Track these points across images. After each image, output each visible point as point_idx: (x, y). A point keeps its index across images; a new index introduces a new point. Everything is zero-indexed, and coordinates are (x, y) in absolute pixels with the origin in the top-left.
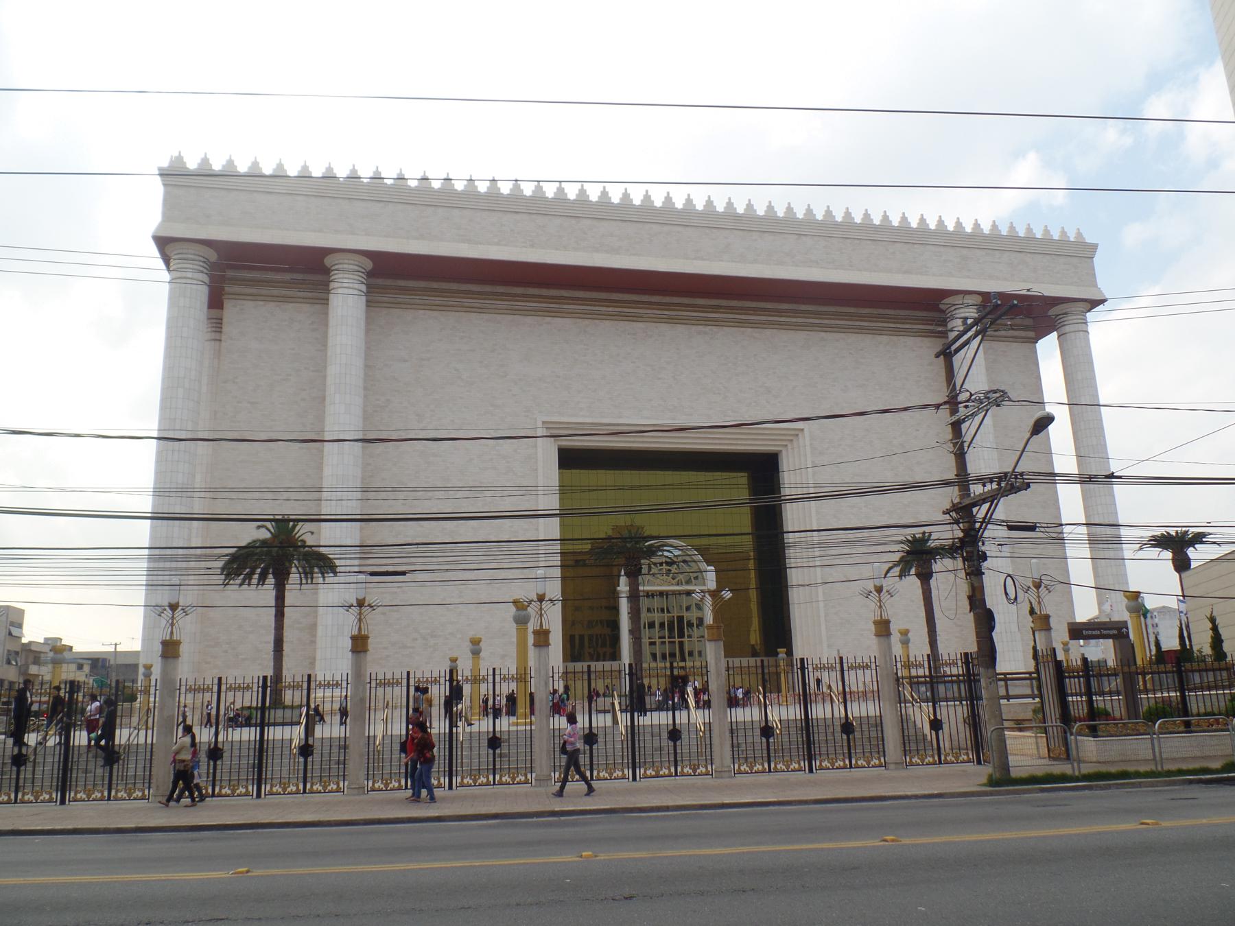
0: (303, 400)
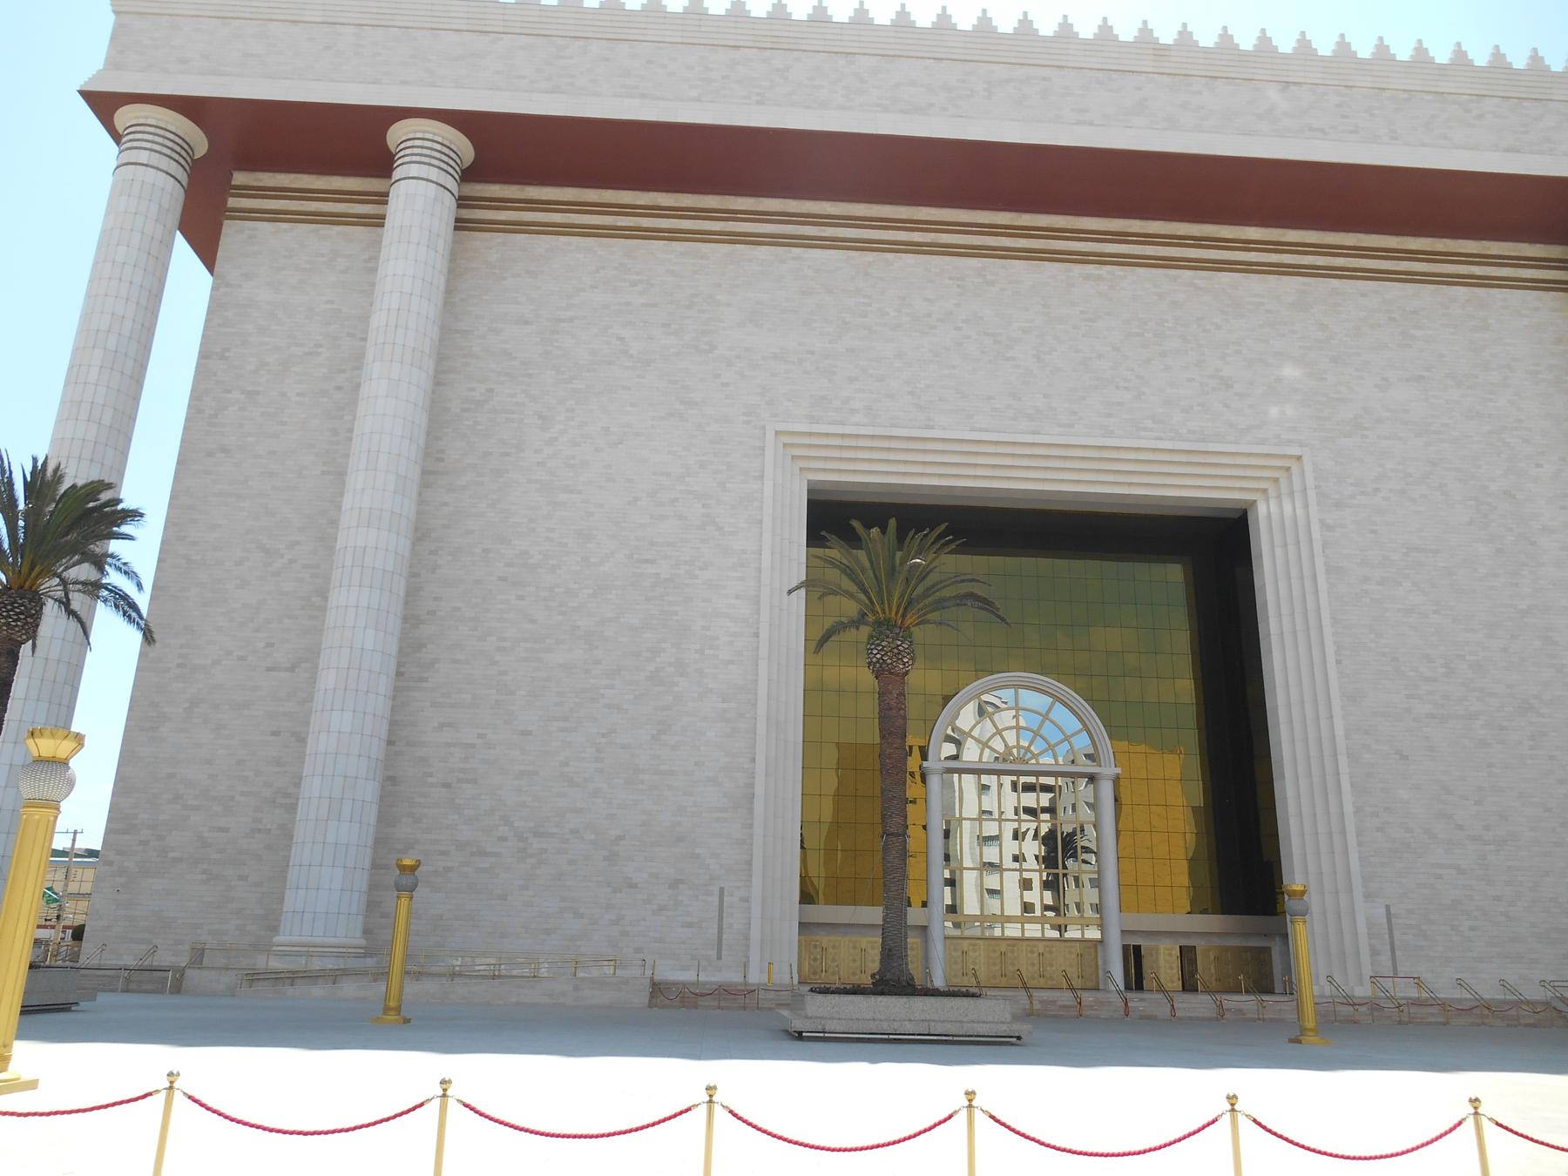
0: (339, 388)
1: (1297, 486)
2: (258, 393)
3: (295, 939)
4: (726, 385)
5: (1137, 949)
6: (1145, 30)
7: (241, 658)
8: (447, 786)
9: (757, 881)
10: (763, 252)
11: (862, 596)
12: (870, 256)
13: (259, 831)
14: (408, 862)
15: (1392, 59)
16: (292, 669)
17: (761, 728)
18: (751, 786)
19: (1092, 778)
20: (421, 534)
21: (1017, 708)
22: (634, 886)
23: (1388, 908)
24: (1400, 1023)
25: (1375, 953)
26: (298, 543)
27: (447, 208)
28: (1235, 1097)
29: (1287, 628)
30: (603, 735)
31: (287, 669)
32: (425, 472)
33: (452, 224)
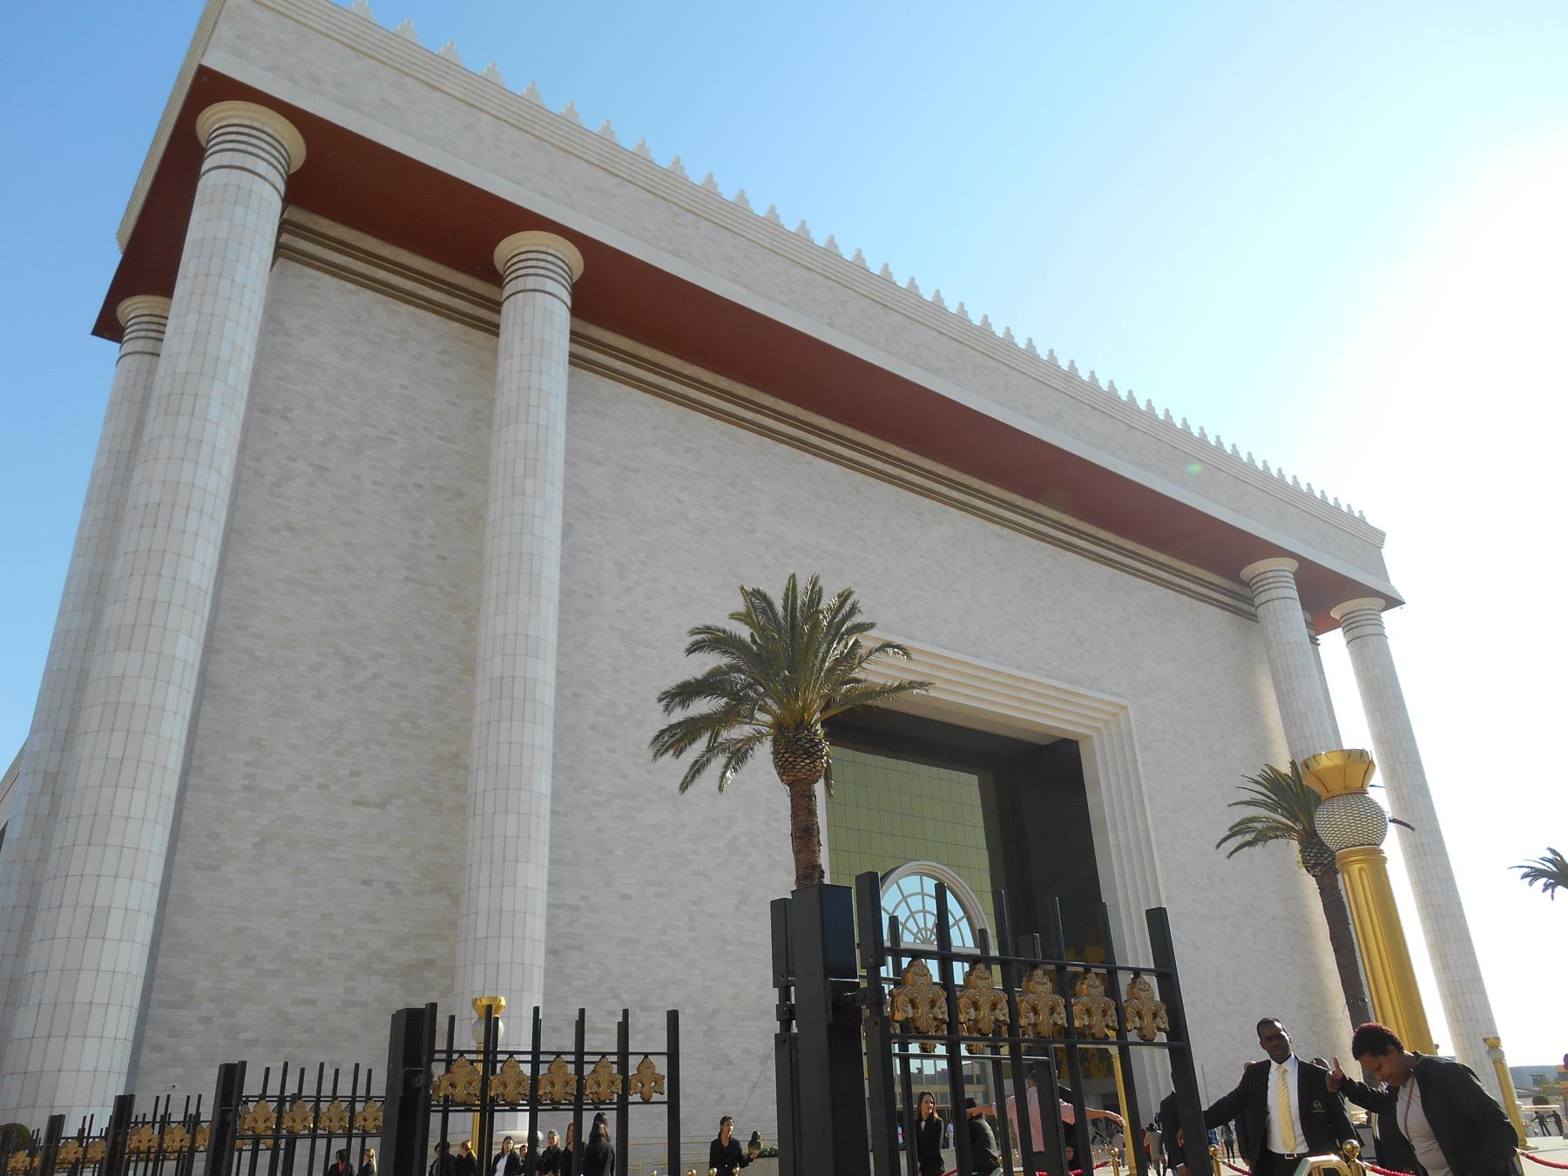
0: (419, 486)
2: (328, 469)
4: (766, 567)
7: (321, 786)
10: (783, 449)
12: (860, 477)
13: (353, 1003)
16: (382, 805)
22: (730, 1063)
26: (382, 656)
30: (694, 903)
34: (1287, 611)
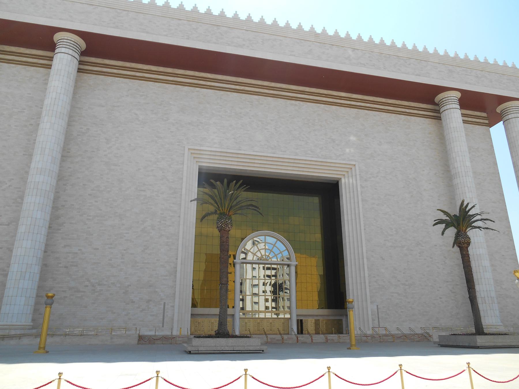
0: (31, 125)
1: (354, 174)
3: (5, 323)
4: (173, 132)
5: (301, 321)
6: (312, 28)
8: (66, 267)
9: (177, 300)
11: (216, 205)
12: (222, 92)
14: (50, 295)
15: (385, 44)
16: (8, 225)
17: (180, 249)
18: (176, 268)
19: (288, 266)
20: (60, 178)
21: (265, 243)
22: (134, 302)
23: (377, 306)
24: (380, 342)
25: (373, 320)
26: (13, 179)
27: (75, 64)
28: (330, 367)
29: (350, 218)
30: (125, 250)
31: (6, 225)
32: (62, 156)
33: (77, 70)
34: (453, 115)
